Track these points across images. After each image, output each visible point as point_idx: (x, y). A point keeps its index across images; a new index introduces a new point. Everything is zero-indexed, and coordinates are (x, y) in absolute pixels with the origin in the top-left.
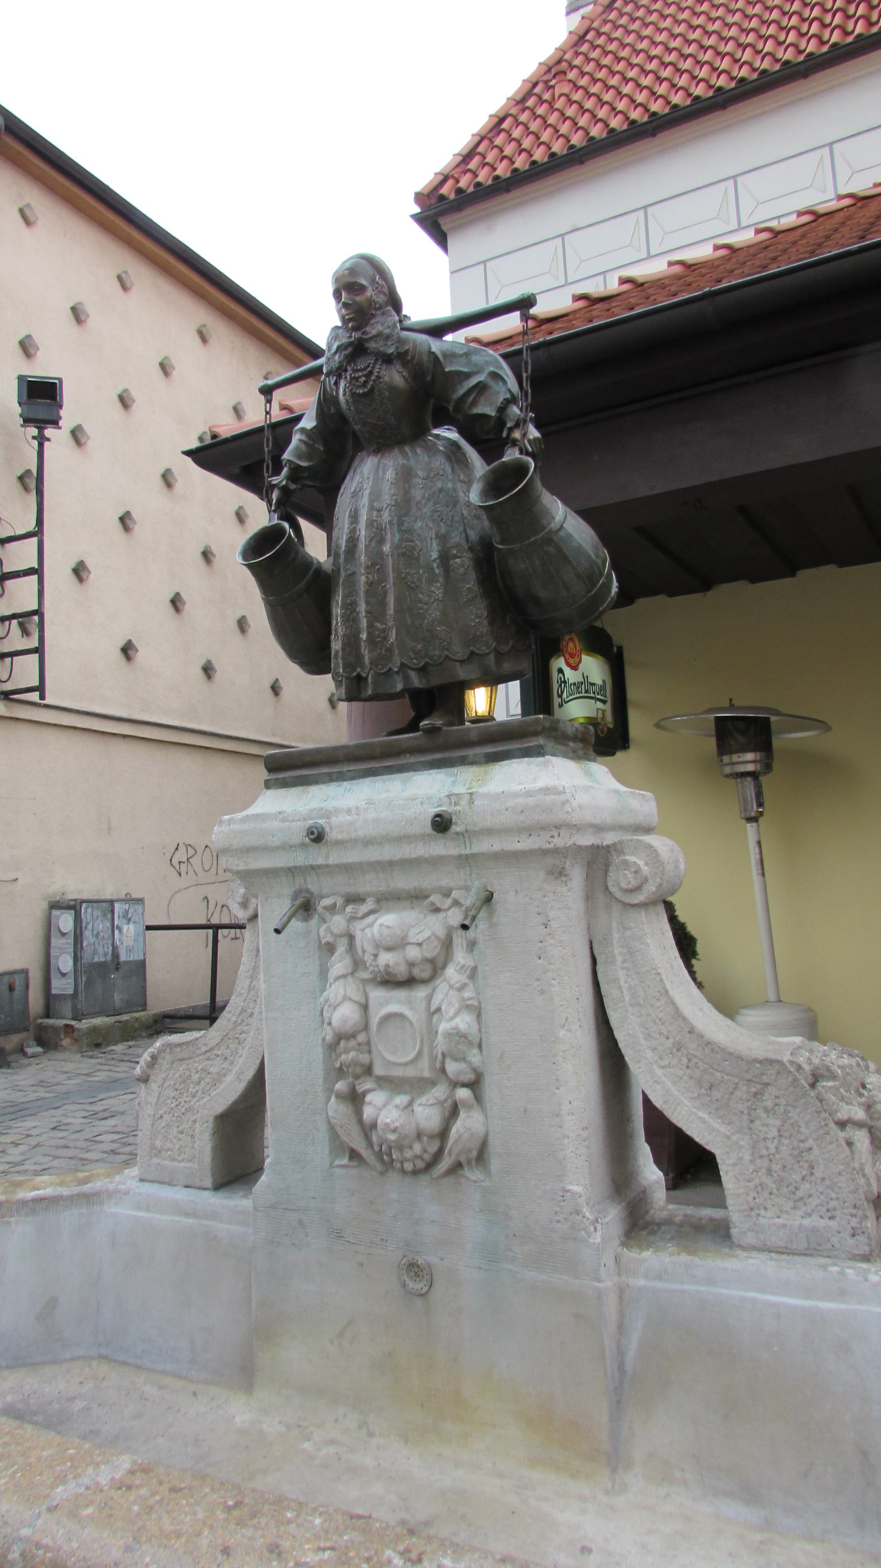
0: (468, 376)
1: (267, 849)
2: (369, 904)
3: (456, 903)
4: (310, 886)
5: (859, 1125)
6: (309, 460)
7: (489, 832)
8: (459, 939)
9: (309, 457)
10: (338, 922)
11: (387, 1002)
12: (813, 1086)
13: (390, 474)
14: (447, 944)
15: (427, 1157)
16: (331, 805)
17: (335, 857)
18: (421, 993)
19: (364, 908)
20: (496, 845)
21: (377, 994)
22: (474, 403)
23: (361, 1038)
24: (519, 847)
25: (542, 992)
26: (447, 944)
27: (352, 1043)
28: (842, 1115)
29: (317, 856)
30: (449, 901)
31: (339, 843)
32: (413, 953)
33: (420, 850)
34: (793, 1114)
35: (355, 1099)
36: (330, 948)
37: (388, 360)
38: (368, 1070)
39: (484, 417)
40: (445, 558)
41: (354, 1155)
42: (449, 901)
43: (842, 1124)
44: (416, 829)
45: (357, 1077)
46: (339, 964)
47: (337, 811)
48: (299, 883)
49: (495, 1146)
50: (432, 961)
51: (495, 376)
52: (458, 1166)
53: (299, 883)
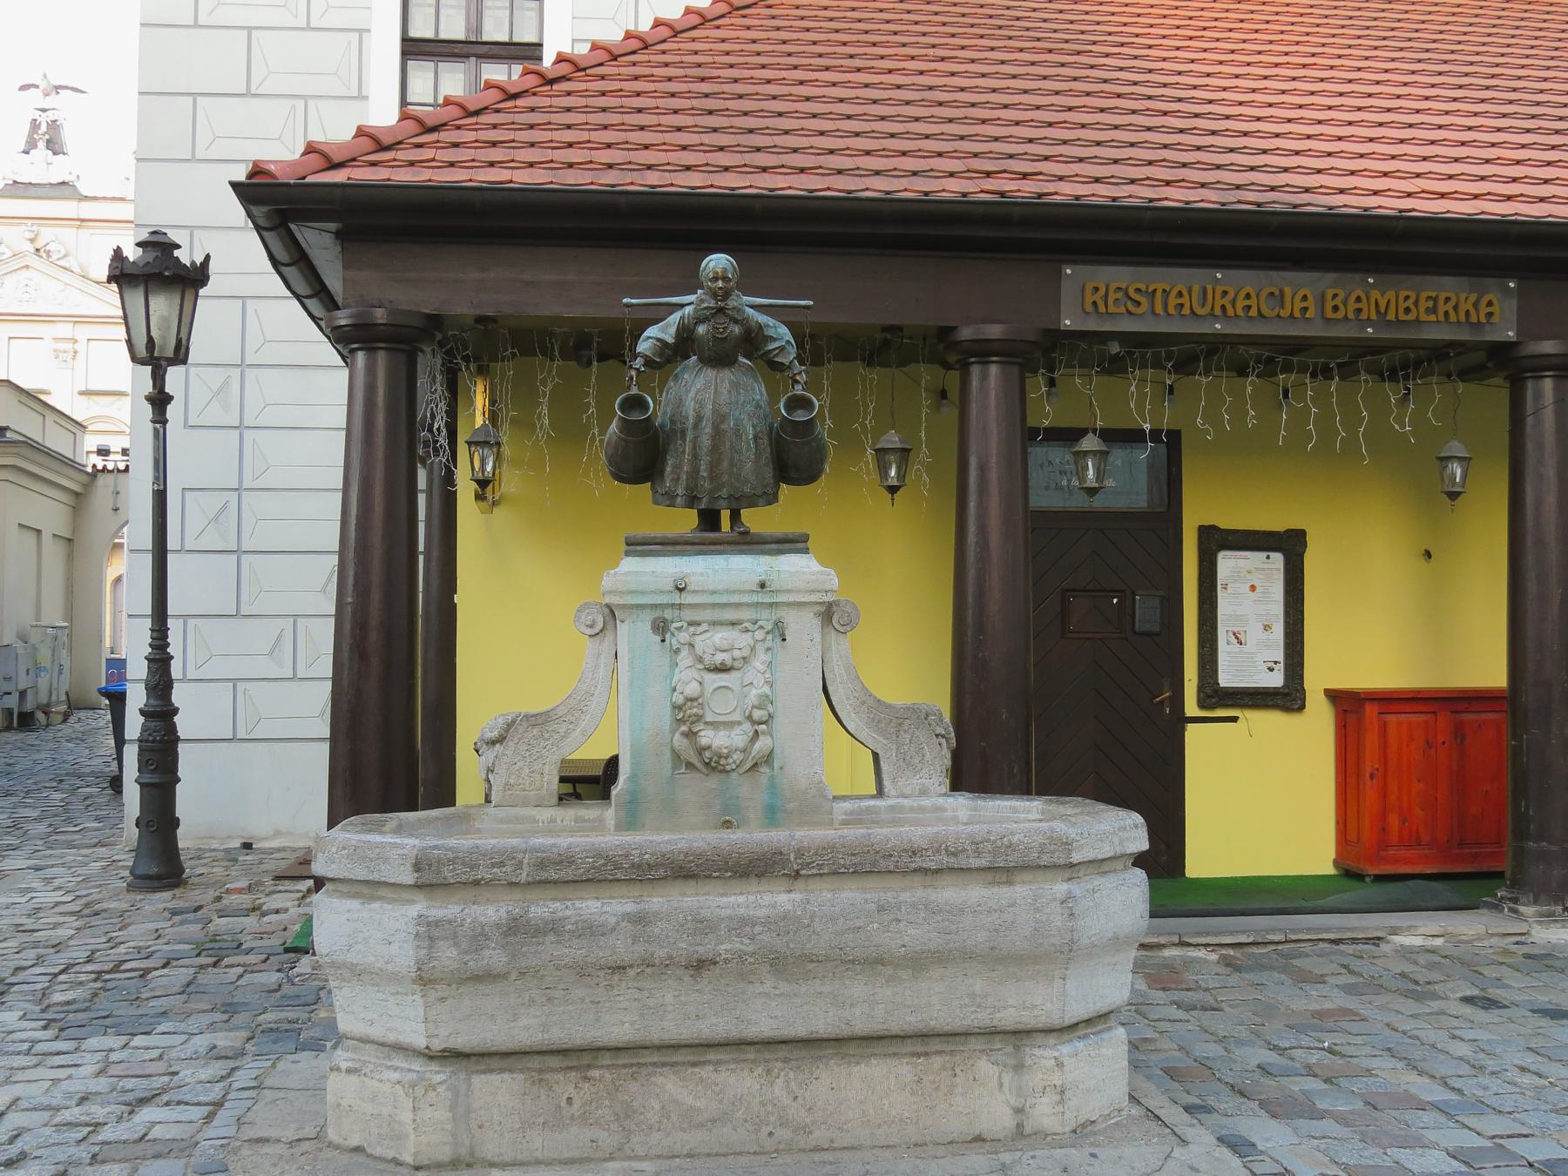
0: (776, 340)
1: (642, 593)
2: (704, 627)
3: (761, 627)
4: (666, 616)
5: (943, 736)
6: (660, 358)
7: (789, 591)
8: (760, 648)
9: (660, 357)
10: (683, 637)
11: (714, 681)
12: (926, 719)
13: (726, 384)
14: (753, 649)
15: (738, 762)
16: (687, 570)
17: (687, 599)
18: (735, 675)
19: (700, 629)
20: (791, 598)
21: (709, 677)
22: (776, 355)
23: (700, 701)
24: (804, 600)
25: (808, 674)
26: (753, 649)
27: (695, 704)
28: (938, 732)
29: (676, 598)
30: (757, 626)
31: (694, 591)
32: (737, 654)
33: (746, 599)
34: (917, 733)
35: (691, 735)
36: (677, 651)
37: (736, 321)
38: (699, 718)
39: (783, 364)
40: (756, 438)
41: (690, 765)
42: (757, 626)
43: (937, 736)
44: (747, 587)
45: (693, 723)
46: (685, 659)
47: (693, 574)
48: (658, 613)
49: (777, 752)
50: (744, 658)
51: (788, 342)
52: (756, 765)
53: (658, 613)
